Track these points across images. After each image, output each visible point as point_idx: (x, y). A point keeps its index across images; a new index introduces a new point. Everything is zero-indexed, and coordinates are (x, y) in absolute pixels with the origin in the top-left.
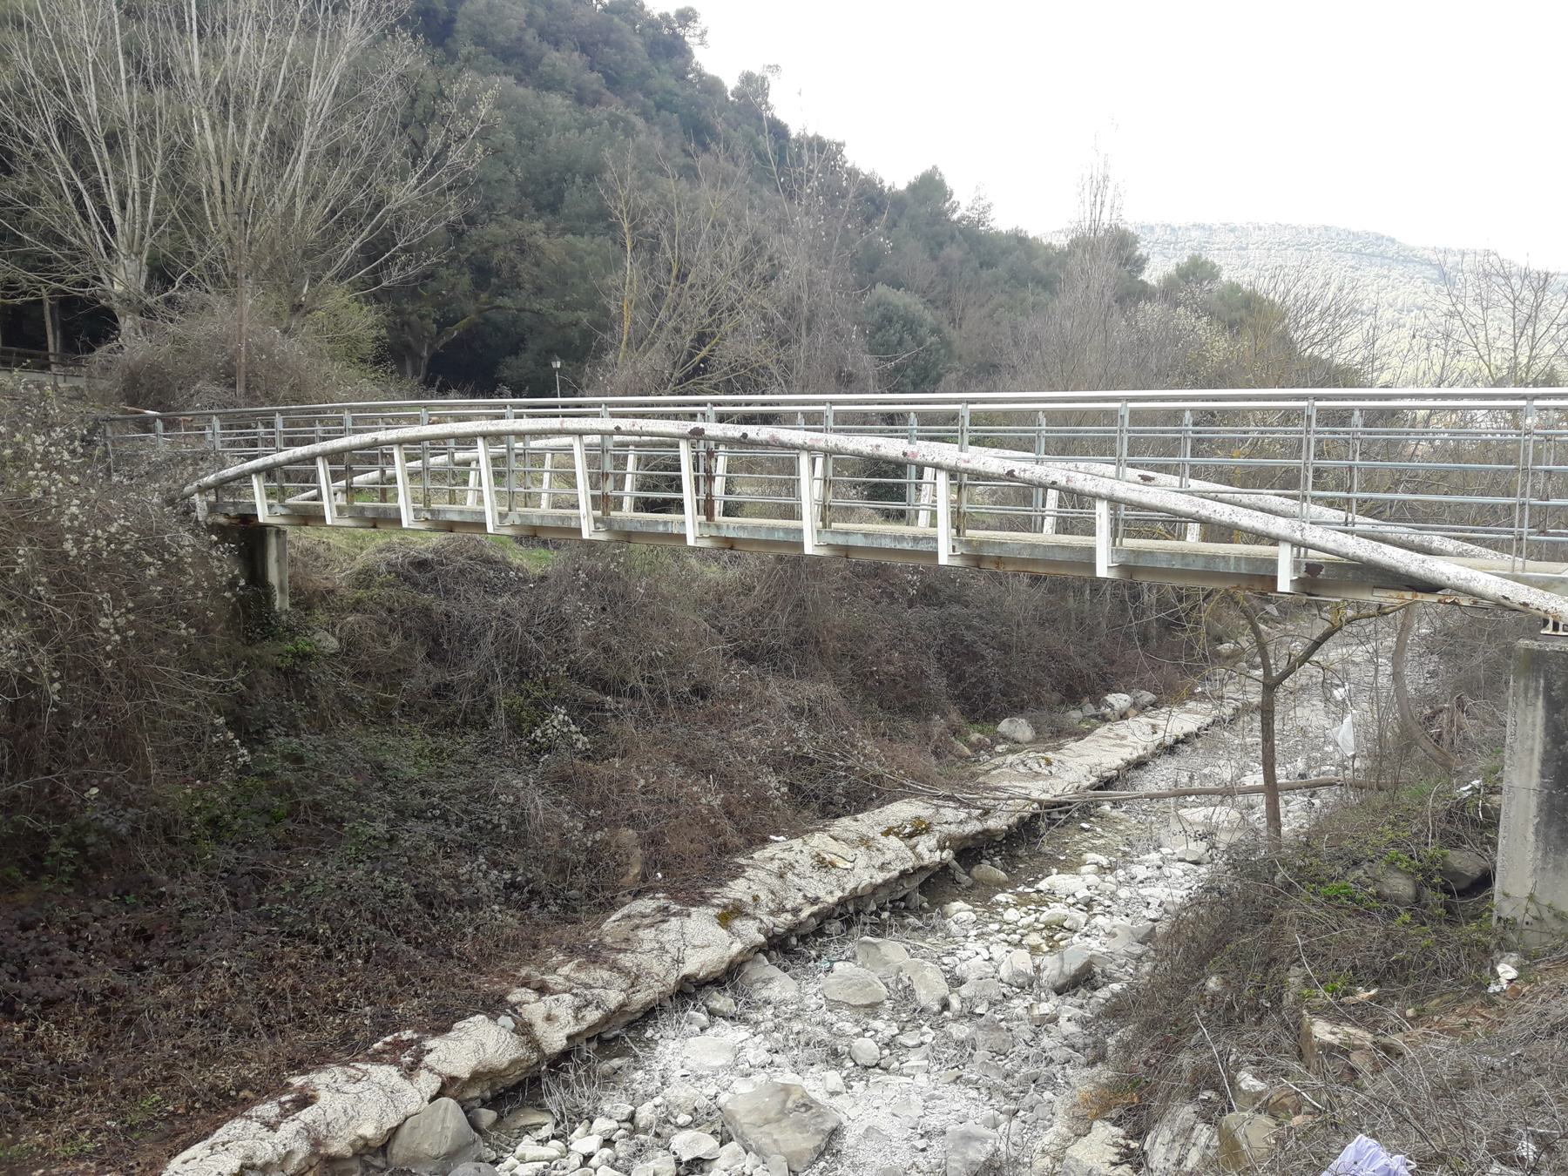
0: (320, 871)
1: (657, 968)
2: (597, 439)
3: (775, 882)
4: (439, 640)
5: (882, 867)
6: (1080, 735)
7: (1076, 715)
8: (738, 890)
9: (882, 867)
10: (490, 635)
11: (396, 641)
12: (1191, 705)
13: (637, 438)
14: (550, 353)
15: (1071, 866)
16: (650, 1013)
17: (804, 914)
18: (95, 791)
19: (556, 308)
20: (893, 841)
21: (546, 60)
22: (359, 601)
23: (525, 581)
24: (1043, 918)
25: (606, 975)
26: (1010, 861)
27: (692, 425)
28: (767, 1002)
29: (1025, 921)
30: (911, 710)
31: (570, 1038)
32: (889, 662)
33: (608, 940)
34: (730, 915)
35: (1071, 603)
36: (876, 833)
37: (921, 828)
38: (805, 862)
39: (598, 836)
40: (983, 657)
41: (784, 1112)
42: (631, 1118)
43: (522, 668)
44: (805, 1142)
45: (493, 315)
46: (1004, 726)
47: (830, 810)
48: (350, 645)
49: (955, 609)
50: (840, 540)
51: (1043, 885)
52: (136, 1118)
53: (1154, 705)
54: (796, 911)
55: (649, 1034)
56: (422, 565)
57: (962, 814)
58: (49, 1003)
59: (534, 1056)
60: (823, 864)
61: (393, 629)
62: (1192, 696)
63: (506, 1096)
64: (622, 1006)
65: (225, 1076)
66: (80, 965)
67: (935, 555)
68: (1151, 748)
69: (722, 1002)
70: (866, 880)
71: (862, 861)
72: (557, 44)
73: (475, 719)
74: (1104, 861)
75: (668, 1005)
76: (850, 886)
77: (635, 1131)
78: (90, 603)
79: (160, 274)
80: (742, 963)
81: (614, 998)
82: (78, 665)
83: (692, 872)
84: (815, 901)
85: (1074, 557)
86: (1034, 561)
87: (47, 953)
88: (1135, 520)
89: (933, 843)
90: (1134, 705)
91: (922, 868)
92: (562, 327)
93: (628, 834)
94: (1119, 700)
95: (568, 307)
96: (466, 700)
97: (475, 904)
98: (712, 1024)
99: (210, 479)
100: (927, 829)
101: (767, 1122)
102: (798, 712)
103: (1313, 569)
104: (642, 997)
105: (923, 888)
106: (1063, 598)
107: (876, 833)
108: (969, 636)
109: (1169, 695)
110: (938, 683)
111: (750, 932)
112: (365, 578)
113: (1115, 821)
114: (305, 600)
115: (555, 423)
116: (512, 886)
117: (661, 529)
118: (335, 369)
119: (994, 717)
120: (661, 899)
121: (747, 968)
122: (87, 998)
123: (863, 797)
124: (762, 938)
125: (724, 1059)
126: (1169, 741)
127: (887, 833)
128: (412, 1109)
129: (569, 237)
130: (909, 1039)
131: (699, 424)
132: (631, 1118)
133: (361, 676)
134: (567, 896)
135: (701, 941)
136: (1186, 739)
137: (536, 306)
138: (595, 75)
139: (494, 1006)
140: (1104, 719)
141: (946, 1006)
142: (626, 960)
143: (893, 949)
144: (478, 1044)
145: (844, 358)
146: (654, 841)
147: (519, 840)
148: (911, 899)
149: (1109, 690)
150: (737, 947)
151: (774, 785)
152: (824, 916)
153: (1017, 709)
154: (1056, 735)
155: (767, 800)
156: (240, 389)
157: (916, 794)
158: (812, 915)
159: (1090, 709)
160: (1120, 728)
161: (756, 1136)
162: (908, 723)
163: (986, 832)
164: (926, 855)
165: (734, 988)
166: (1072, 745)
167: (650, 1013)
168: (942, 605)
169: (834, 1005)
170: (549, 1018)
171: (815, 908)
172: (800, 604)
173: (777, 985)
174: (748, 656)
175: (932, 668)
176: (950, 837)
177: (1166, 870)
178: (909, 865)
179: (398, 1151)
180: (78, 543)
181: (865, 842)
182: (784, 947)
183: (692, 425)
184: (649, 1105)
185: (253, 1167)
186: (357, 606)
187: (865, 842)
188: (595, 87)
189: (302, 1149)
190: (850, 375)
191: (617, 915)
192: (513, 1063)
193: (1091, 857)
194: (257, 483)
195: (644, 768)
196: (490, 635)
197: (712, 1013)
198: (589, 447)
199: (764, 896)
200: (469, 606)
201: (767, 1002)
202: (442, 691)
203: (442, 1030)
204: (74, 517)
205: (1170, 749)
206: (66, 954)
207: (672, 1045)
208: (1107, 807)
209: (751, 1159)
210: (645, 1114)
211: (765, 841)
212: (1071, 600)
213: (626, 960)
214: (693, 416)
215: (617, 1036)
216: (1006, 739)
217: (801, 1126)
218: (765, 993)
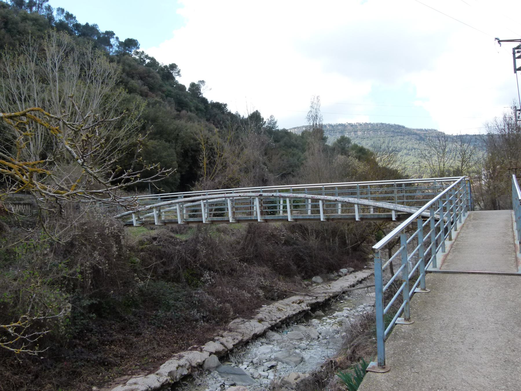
0: (161, 313)
1: (247, 332)
2: (231, 198)
5: (294, 310)
6: (335, 280)
7: (333, 275)
8: (260, 316)
9: (294, 310)
10: (176, 257)
12: (364, 271)
13: (191, 204)
15: (341, 310)
17: (278, 321)
18: (112, 292)
20: (295, 305)
21: (130, 83)
22: (142, 249)
23: (181, 242)
24: (337, 320)
26: (324, 311)
27: (259, 194)
28: (274, 340)
29: (332, 322)
31: (234, 345)
32: (281, 261)
33: (232, 327)
34: (261, 321)
35: (327, 243)
36: (290, 303)
37: (301, 302)
38: (275, 310)
40: (305, 260)
42: (252, 362)
44: (298, 359)
46: (314, 279)
47: (273, 300)
49: (295, 246)
50: (296, 218)
51: (334, 315)
52: (143, 362)
53: (354, 271)
54: (275, 321)
55: (248, 347)
57: (311, 298)
58: (112, 341)
59: (226, 350)
60: (279, 310)
62: (364, 269)
64: (242, 340)
65: (160, 354)
68: (356, 282)
69: (264, 340)
70: (291, 313)
72: (133, 78)
73: (177, 279)
75: (250, 341)
76: (287, 315)
81: (240, 338)
83: (248, 312)
84: (280, 318)
86: (341, 219)
87: (106, 331)
88: (364, 208)
89: (305, 305)
90: (348, 272)
91: (304, 311)
93: (228, 305)
94: (344, 270)
96: (172, 275)
97: (197, 321)
98: (263, 345)
99: (119, 215)
100: (303, 302)
101: (287, 357)
102: (259, 275)
103: (399, 215)
104: (245, 338)
106: (325, 242)
107: (290, 303)
108: (301, 254)
109: (357, 268)
110: (294, 267)
112: (141, 243)
116: (203, 317)
119: (310, 277)
120: (241, 319)
121: (267, 333)
122: (120, 341)
123: (282, 296)
124: (270, 326)
125: (269, 350)
126: (360, 280)
127: (293, 303)
130: (312, 343)
131: (261, 193)
132: (252, 362)
134: (219, 320)
136: (364, 279)
138: (146, 87)
139: (213, 340)
140: (340, 276)
141: (319, 338)
143: (302, 327)
144: (212, 346)
145: (264, 175)
146: (234, 306)
147: (203, 306)
148: (304, 317)
149: (341, 268)
150: (265, 327)
151: (261, 293)
152: (282, 322)
153: (316, 274)
154: (330, 280)
157: (296, 295)
158: (280, 321)
159: (336, 274)
160: (346, 277)
161: (284, 360)
163: (318, 302)
164: (304, 307)
168: (291, 245)
169: (292, 339)
170: (227, 341)
171: (280, 320)
172: (256, 245)
173: (276, 336)
175: (291, 263)
176: (309, 304)
178: (300, 310)
179: (206, 366)
180: (109, 230)
181: (287, 305)
182: (276, 328)
183: (259, 194)
186: (142, 250)
187: (287, 305)
188: (146, 91)
189: (188, 364)
190: (266, 180)
192: (223, 350)
194: (133, 215)
196: (176, 257)
197: (262, 343)
198: (231, 200)
199: (267, 317)
201: (274, 340)
202: (166, 272)
203: (204, 344)
204: (107, 224)
205: (360, 282)
207: (255, 349)
208: (347, 297)
209: (284, 365)
210: (255, 361)
211: (261, 307)
212: (327, 243)
213: (239, 330)
214: (259, 192)
216: (315, 282)
217: (295, 356)
218: (273, 338)
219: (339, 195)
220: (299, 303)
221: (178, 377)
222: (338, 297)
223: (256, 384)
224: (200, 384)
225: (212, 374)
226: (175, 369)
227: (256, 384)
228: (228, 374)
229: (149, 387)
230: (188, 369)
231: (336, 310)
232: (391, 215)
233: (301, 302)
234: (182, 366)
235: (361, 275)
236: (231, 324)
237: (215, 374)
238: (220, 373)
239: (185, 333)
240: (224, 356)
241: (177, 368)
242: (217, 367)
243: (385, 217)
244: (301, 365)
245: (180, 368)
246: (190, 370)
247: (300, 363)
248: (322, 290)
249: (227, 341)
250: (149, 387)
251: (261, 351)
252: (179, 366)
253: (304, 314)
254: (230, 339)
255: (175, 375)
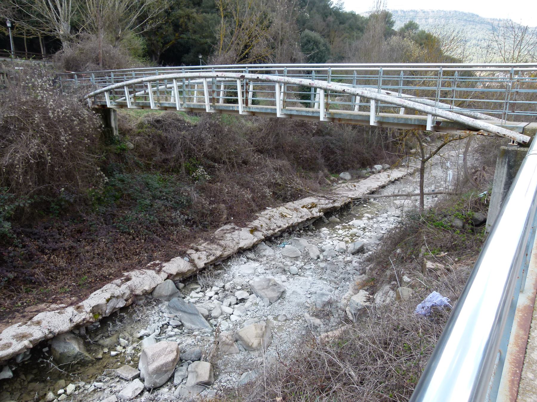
0: (130, 214)
1: (231, 245)
3: (268, 221)
4: (164, 145)
5: (301, 217)
6: (365, 178)
7: (364, 171)
8: (256, 223)
9: (301, 217)
10: (180, 143)
11: (151, 145)
12: (400, 168)
14: (198, 53)
15: (360, 218)
16: (229, 258)
18: (63, 189)
19: (200, 38)
20: (305, 210)
22: (139, 133)
23: (190, 127)
24: (350, 233)
25: (216, 246)
26: (341, 216)
28: (265, 256)
30: (312, 169)
31: (205, 264)
32: (306, 154)
33: (217, 237)
34: (253, 230)
35: (365, 136)
36: (300, 207)
37: (314, 206)
38: (277, 215)
39: (213, 206)
40: (336, 153)
41: (268, 286)
42: (224, 287)
43: (189, 153)
44: (275, 295)
45: (180, 40)
46: (342, 175)
47: (285, 200)
48: (137, 146)
49: (328, 137)
50: (289, 113)
51: (351, 223)
52: (81, 282)
54: (274, 230)
55: (229, 263)
56: (158, 121)
57: (327, 202)
59: (195, 269)
60: (283, 216)
61: (150, 141)
62: (402, 166)
63: (187, 280)
64: (221, 255)
65: (105, 272)
66: (62, 240)
67: (319, 118)
68: (387, 182)
69: (251, 255)
71: (295, 215)
73: (175, 170)
74: (370, 216)
75: (235, 256)
76: (291, 223)
77: (225, 290)
78: (58, 132)
79: (74, 28)
80: (257, 244)
81: (218, 253)
82: (55, 151)
83: (242, 216)
84: (280, 227)
85: (364, 119)
86: (351, 120)
87: (52, 236)
88: (384, 107)
89: (317, 210)
90: (383, 169)
91: (314, 218)
92: (202, 44)
93: (223, 206)
94: (378, 167)
95: (205, 37)
96: (173, 164)
97: (177, 225)
99: (92, 93)
100: (316, 206)
101: (264, 289)
102: (276, 170)
104: (226, 253)
105: (314, 224)
106: (363, 134)
107: (300, 207)
108: (332, 146)
109: (394, 165)
110: (321, 161)
111: (260, 235)
112: (141, 125)
113: (374, 204)
114: (123, 132)
115: (197, 74)
116: (188, 220)
117: (231, 109)
118: (130, 59)
119: (339, 172)
120: (233, 225)
121: (259, 246)
122: (65, 249)
123: (296, 196)
124: (263, 237)
125: (251, 271)
126: (393, 180)
127: (303, 207)
128: (159, 282)
129: (204, 14)
130: (307, 267)
131: (243, 74)
132: (224, 287)
133: (141, 156)
134: (205, 223)
135: (244, 237)
136: (398, 180)
137: (194, 37)
139: (183, 254)
140: (373, 173)
141: (319, 258)
142: (222, 242)
143: (303, 241)
144: (178, 265)
145: (293, 53)
146: (230, 208)
147: (190, 207)
148: (310, 226)
149: (376, 164)
150: (256, 240)
152: (283, 231)
153: (346, 169)
154: (359, 177)
155: (266, 197)
156: (101, 65)
157: (313, 195)
158: (279, 231)
159: (369, 170)
160: (378, 176)
161: (260, 293)
162: (311, 174)
163: (334, 207)
164: (315, 214)
165: (255, 251)
166: (363, 181)
167: (229, 258)
168: (323, 136)
169: (285, 257)
170: (199, 258)
171: (280, 229)
172: (277, 135)
173: (268, 251)
174: (260, 151)
175: (319, 156)
176: (323, 209)
177: (389, 219)
178: (309, 217)
179: (155, 294)
180: (53, 113)
181: (296, 210)
182: (270, 240)
184: (229, 283)
185: (114, 297)
186: (139, 134)
187: (296, 210)
189: (128, 292)
190: (295, 59)
191: (219, 230)
192: (189, 270)
193: (366, 215)
194: (106, 94)
195: (228, 186)
196: (180, 143)
197: (248, 258)
198: (208, 82)
199: (264, 225)
200: (172, 134)
201: (265, 256)
202: (165, 161)
203: (168, 261)
204: (51, 105)
205: (393, 182)
206: (58, 236)
207: (236, 267)
208: (372, 200)
209: (258, 299)
210: (228, 286)
212: (365, 135)
213: (222, 242)
214: (242, 72)
215: (219, 264)
216: (342, 179)
217: (274, 290)
218: (264, 253)
219: (360, 82)
220: (310, 208)
221: (107, 312)
222: (357, 202)
223: (207, 330)
224: (139, 320)
225: (160, 306)
226: (103, 301)
227: (207, 330)
228: (177, 310)
229: (50, 332)
230: (126, 300)
231: (355, 216)
232: (425, 121)
233: (314, 206)
234: (118, 297)
235: (396, 174)
236: (218, 232)
237: (163, 307)
238: (169, 307)
239: (157, 239)
240: (187, 280)
241: (108, 301)
242: (169, 297)
243: (416, 123)
244: (276, 304)
245: (114, 300)
246: (130, 300)
247: (276, 301)
248: (348, 189)
249: (199, 258)
250: (50, 332)
251: (242, 271)
252: (112, 297)
253: (314, 220)
254: (203, 255)
255: (104, 308)
